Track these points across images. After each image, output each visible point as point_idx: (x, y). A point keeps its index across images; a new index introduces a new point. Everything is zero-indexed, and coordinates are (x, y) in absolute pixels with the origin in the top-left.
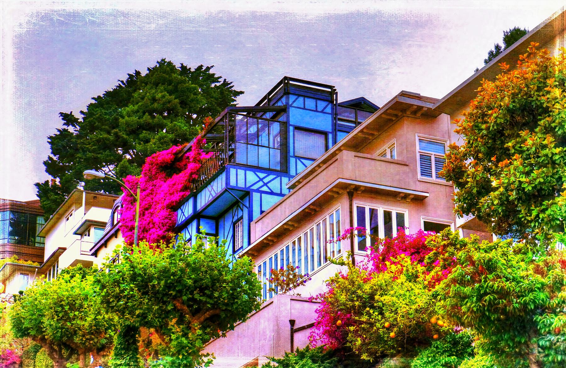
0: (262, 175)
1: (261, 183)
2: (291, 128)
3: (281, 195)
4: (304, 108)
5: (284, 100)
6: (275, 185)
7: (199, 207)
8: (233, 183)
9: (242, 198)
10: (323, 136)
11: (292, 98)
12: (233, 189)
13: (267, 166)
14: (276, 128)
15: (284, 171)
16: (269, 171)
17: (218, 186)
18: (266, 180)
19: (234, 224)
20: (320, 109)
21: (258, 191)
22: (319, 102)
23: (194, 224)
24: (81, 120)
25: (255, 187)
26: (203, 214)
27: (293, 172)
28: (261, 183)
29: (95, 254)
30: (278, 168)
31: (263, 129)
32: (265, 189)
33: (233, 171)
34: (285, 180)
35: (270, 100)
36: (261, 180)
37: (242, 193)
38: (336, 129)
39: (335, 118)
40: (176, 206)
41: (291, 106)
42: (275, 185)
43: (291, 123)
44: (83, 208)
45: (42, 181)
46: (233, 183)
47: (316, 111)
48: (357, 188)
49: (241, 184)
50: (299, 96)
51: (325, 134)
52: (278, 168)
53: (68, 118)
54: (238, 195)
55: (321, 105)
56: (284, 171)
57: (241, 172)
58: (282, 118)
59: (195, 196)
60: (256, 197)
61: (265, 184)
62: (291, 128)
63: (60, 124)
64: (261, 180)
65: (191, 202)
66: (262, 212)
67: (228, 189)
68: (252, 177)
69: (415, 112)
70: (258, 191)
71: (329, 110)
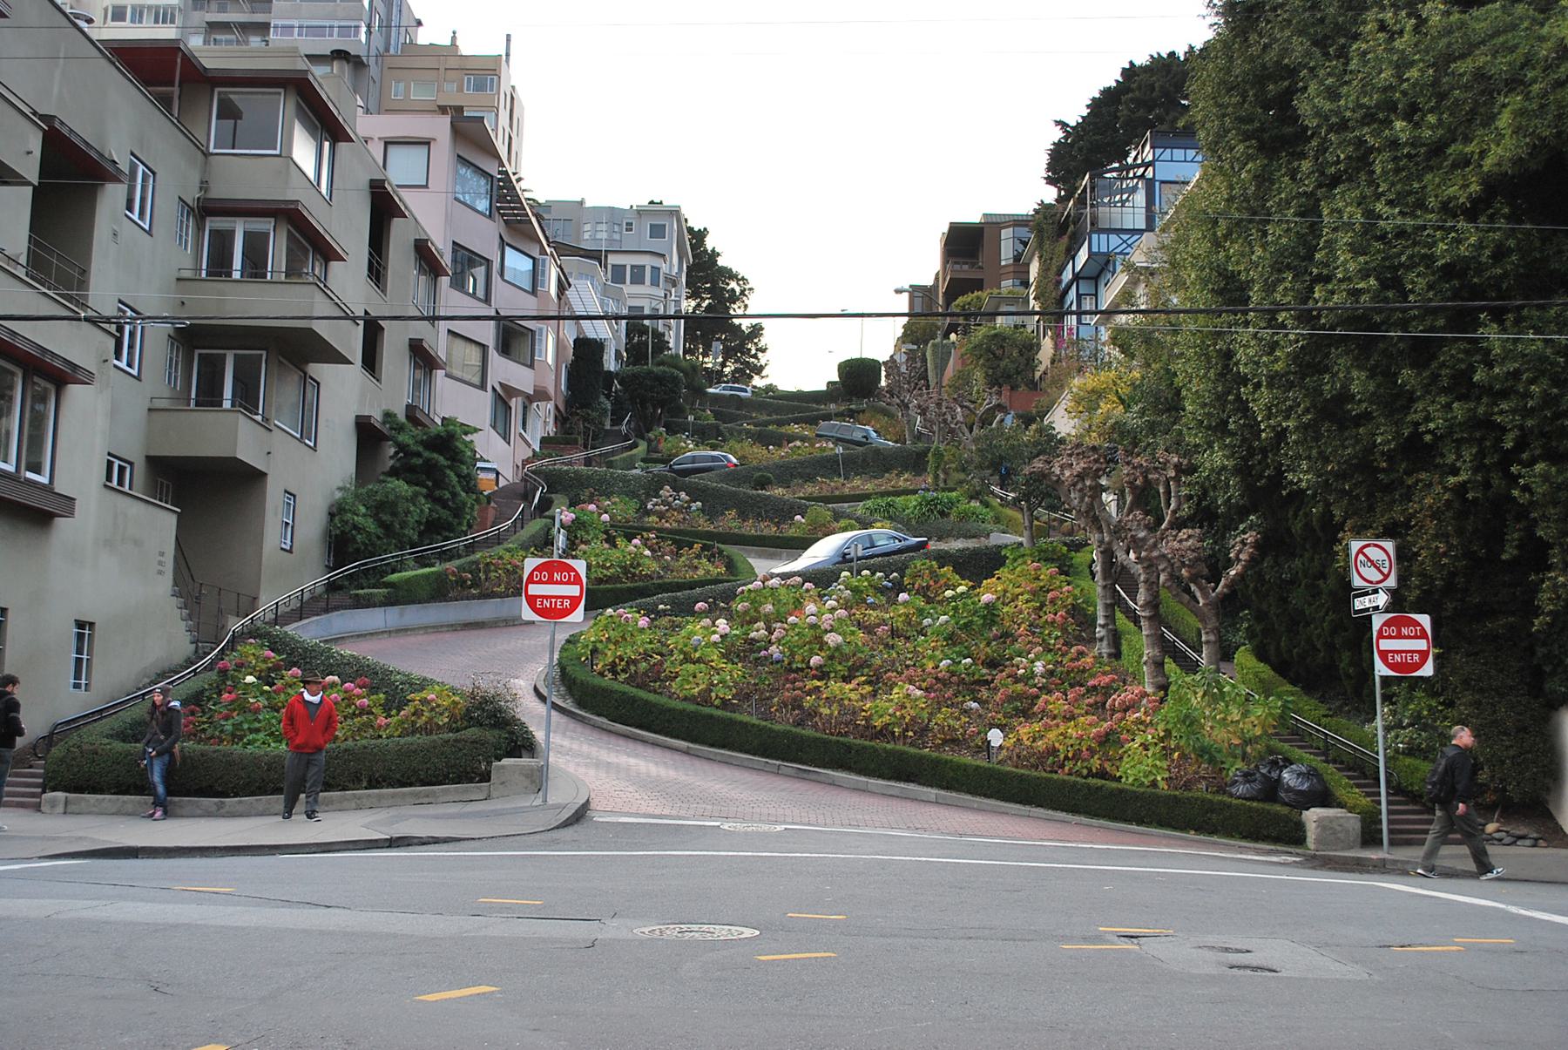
0: (1125, 237)
1: (1125, 245)
2: (1157, 184)
4: (1172, 161)
7: (1078, 269)
8: (1095, 249)
11: (1159, 151)
12: (1096, 254)
18: (1129, 242)
20: (1189, 159)
25: (1118, 250)
26: (1081, 275)
28: (1125, 245)
33: (1095, 237)
36: (1125, 242)
41: (1157, 160)
43: (1157, 178)
46: (1095, 249)
47: (1185, 161)
50: (1166, 148)
54: (1102, 260)
55: (1191, 153)
57: (1103, 237)
58: (1149, 173)
61: (1129, 246)
62: (1157, 184)
64: (1125, 242)
68: (1115, 240)
70: (1121, 253)
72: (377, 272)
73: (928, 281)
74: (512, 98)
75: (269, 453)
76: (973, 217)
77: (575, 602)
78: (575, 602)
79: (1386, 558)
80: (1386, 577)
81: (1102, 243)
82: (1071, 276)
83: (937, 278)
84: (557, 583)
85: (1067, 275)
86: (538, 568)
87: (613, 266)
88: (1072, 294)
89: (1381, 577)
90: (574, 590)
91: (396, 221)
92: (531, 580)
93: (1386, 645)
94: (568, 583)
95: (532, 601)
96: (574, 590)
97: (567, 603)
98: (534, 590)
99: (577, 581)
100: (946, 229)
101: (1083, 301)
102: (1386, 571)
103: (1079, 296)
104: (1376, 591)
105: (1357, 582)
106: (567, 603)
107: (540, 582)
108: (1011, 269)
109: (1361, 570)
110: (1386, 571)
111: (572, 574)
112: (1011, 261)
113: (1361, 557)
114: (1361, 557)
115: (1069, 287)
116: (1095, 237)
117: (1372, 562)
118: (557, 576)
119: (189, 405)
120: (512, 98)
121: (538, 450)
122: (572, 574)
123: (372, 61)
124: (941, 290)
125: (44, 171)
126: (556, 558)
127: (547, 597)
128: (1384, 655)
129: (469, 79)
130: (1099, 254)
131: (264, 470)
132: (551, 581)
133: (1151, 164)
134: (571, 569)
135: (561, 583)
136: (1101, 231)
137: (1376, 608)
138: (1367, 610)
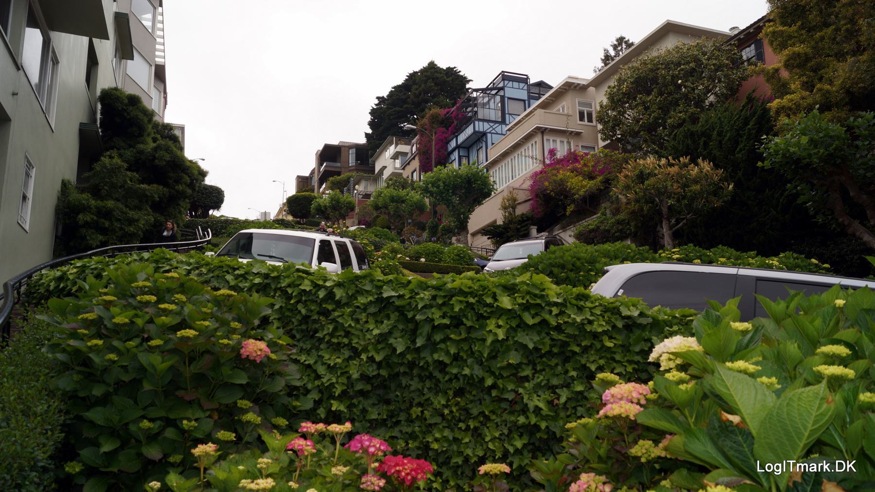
0: (492, 124)
1: (491, 129)
3: (502, 134)
5: (502, 83)
6: (498, 130)
7: (459, 143)
8: (477, 129)
9: (482, 136)
10: (523, 103)
11: (506, 82)
13: (494, 119)
14: (498, 98)
15: (503, 122)
16: (495, 122)
17: (469, 130)
19: (478, 150)
21: (490, 133)
22: (521, 84)
23: (457, 151)
25: (488, 131)
26: (462, 146)
27: (507, 123)
28: (491, 129)
29: (404, 169)
30: (500, 120)
31: (492, 98)
32: (493, 131)
33: (477, 123)
34: (504, 126)
35: (494, 84)
37: (481, 134)
38: (530, 98)
39: (529, 93)
42: (498, 130)
44: (393, 146)
46: (477, 129)
48: (546, 129)
49: (481, 130)
50: (510, 81)
51: (524, 101)
52: (500, 120)
55: (522, 85)
56: (503, 122)
57: (481, 123)
58: (501, 93)
59: (457, 137)
60: (489, 135)
65: (455, 140)
66: (493, 144)
67: (475, 132)
68: (486, 126)
69: (575, 87)
70: (490, 133)
71: (526, 88)
73: (307, 174)
75: (14, 94)
76: (335, 142)
81: (481, 127)
82: (455, 145)
83: (313, 172)
85: (453, 144)
88: (455, 155)
100: (321, 148)
103: (460, 157)
108: (354, 168)
112: (354, 164)
115: (454, 150)
116: (477, 123)
124: (316, 178)
130: (479, 132)
133: (502, 89)
136: (480, 120)
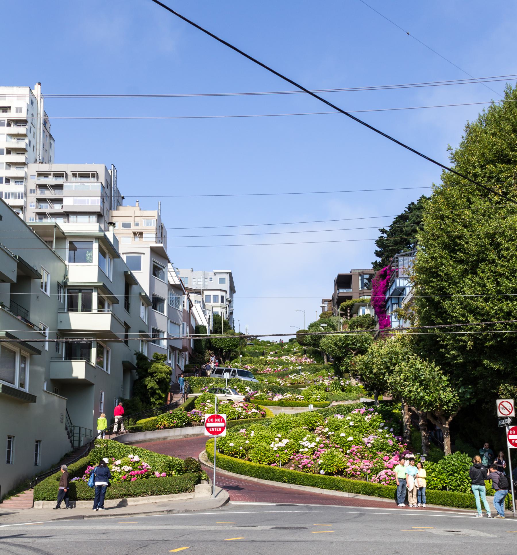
7: (391, 293)
21: (408, 287)
24: (388, 230)
25: (407, 286)
33: (398, 281)
40: (384, 293)
45: (374, 261)
46: (398, 285)
49: (401, 285)
53: (383, 231)
57: (401, 281)
63: (380, 234)
70: (408, 287)
72: (127, 306)
74: (162, 228)
77: (223, 428)
78: (223, 428)
79: (510, 406)
80: (511, 413)
84: (216, 422)
85: (387, 296)
86: (210, 417)
87: (206, 296)
88: (389, 303)
89: (509, 413)
90: (222, 425)
91: (134, 287)
92: (207, 422)
93: (511, 437)
94: (221, 422)
95: (208, 428)
96: (222, 425)
97: (220, 429)
98: (208, 425)
99: (223, 421)
101: (394, 306)
102: (510, 411)
103: (392, 304)
104: (507, 418)
105: (500, 415)
106: (220, 429)
107: (211, 422)
109: (501, 410)
110: (510, 411)
111: (222, 419)
113: (501, 406)
114: (501, 406)
117: (505, 408)
118: (216, 420)
119: (62, 360)
120: (162, 228)
121: (183, 370)
122: (222, 419)
123: (105, 215)
125: (19, 277)
126: (216, 413)
127: (213, 427)
128: (511, 441)
129: (145, 222)
130: (399, 288)
131: (93, 383)
132: (214, 422)
134: (221, 417)
135: (218, 422)
137: (507, 424)
138: (504, 425)
